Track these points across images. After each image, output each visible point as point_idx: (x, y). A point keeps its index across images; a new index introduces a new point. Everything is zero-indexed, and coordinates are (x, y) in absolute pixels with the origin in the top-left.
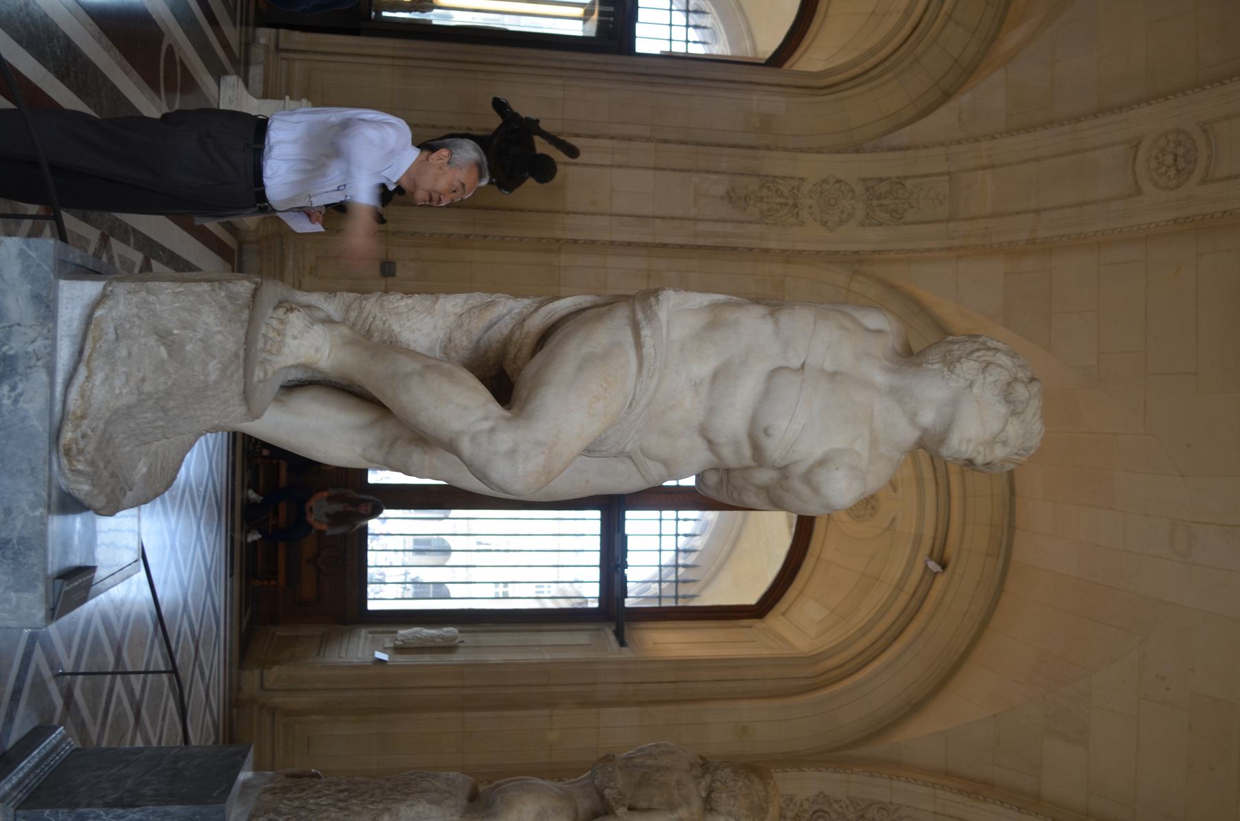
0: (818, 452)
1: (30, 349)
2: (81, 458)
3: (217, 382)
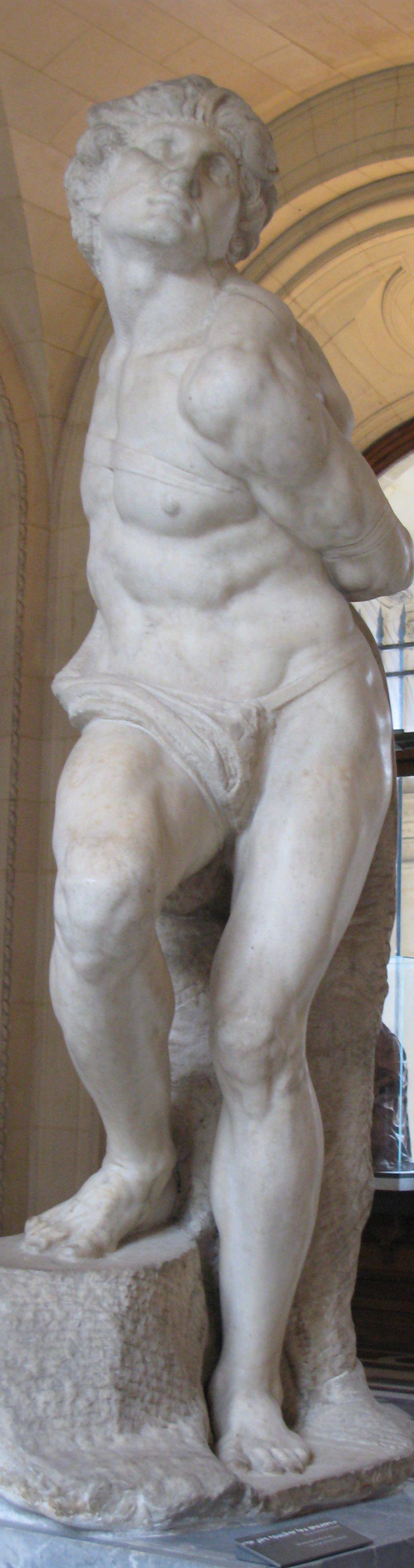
0: (184, 429)
2: (72, 1493)
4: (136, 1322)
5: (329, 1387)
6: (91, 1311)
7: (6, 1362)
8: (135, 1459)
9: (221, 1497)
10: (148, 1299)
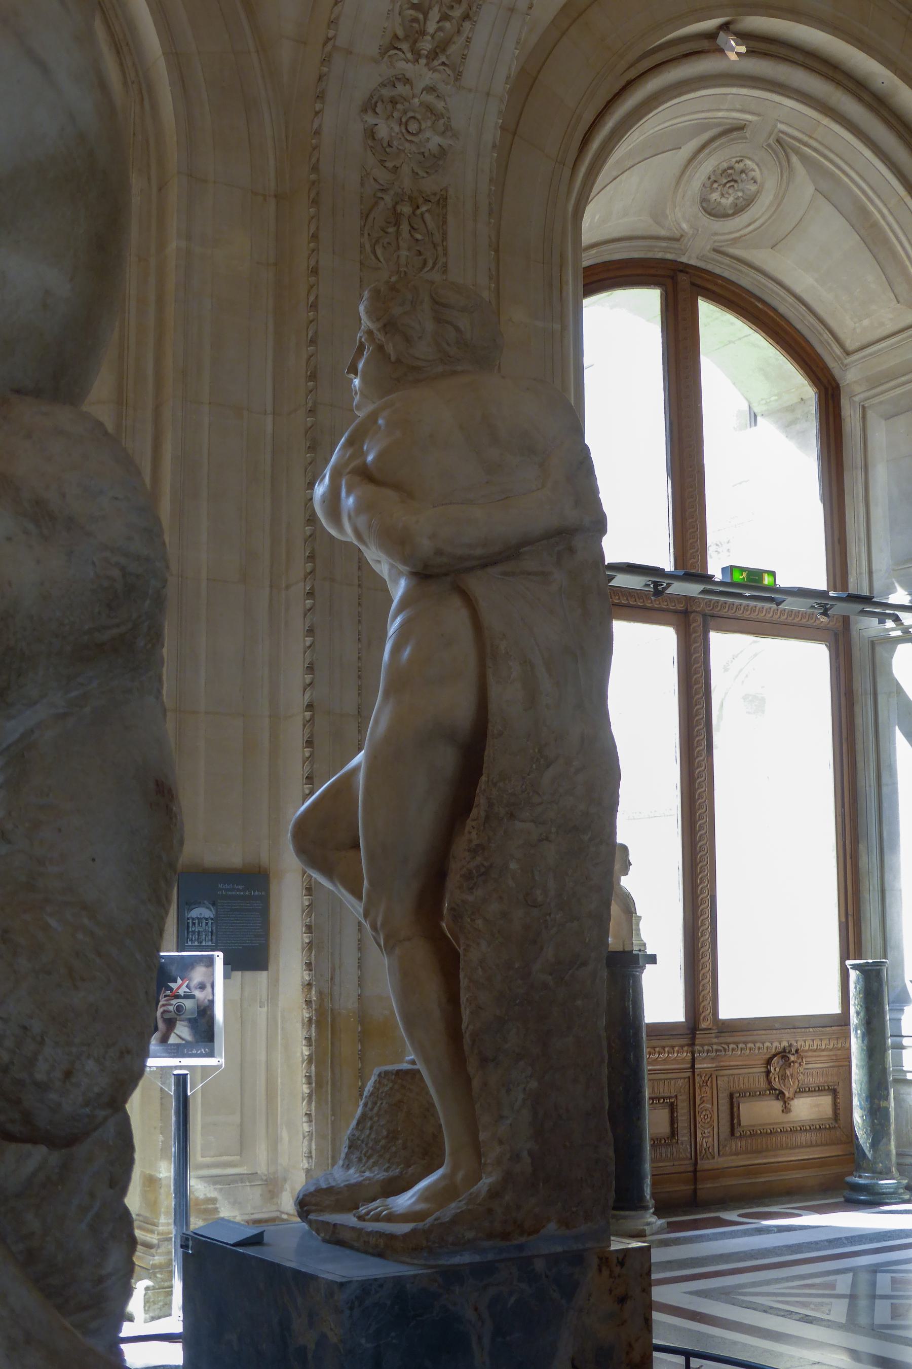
4: (375, 1103)
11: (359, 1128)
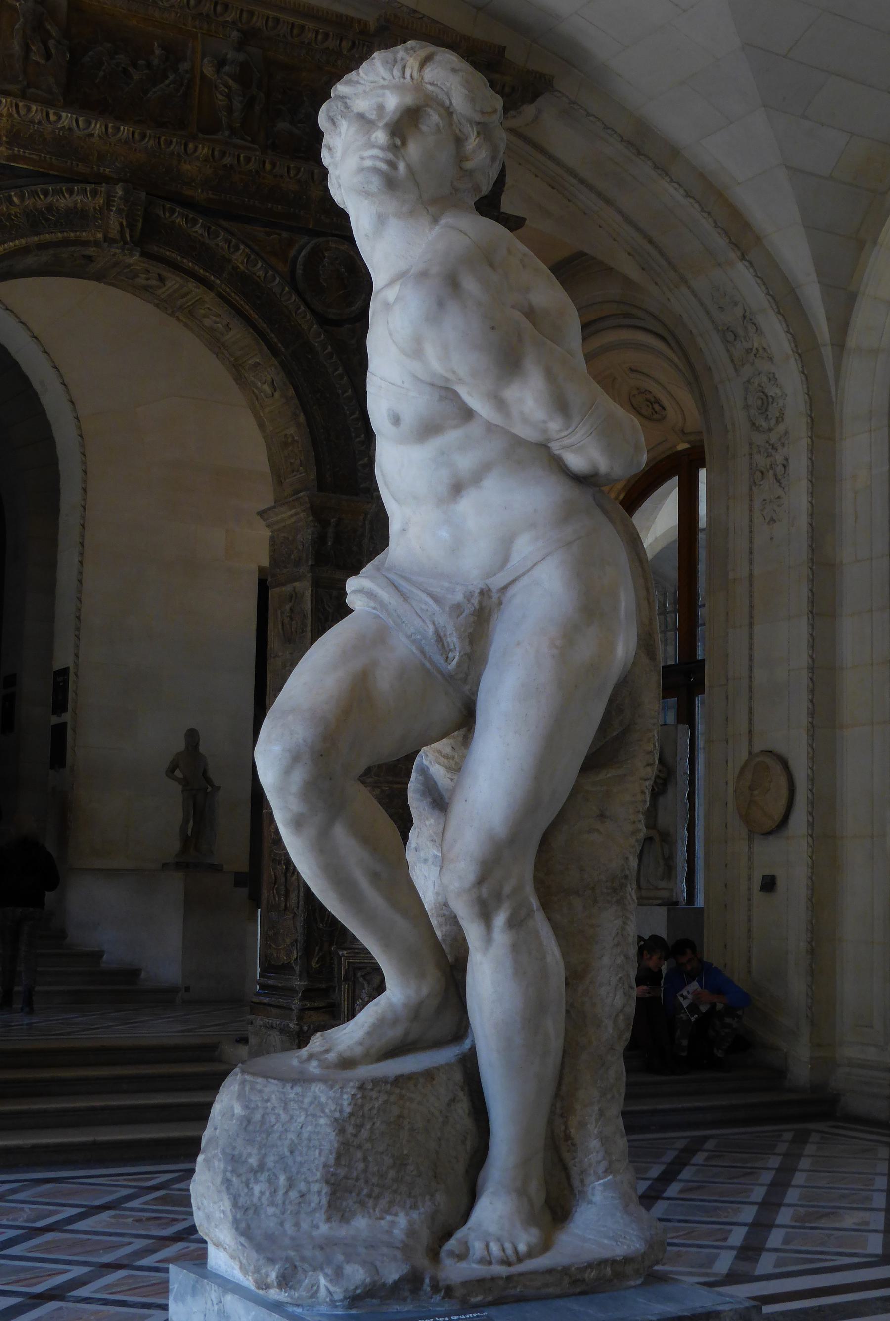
1: (216, 1307)
3: (246, 1107)
4: (359, 1127)
5: (594, 1188)
6: (314, 1115)
7: (233, 1156)
8: (326, 1245)
9: (396, 1283)
10: (376, 1106)
11: (343, 1163)
